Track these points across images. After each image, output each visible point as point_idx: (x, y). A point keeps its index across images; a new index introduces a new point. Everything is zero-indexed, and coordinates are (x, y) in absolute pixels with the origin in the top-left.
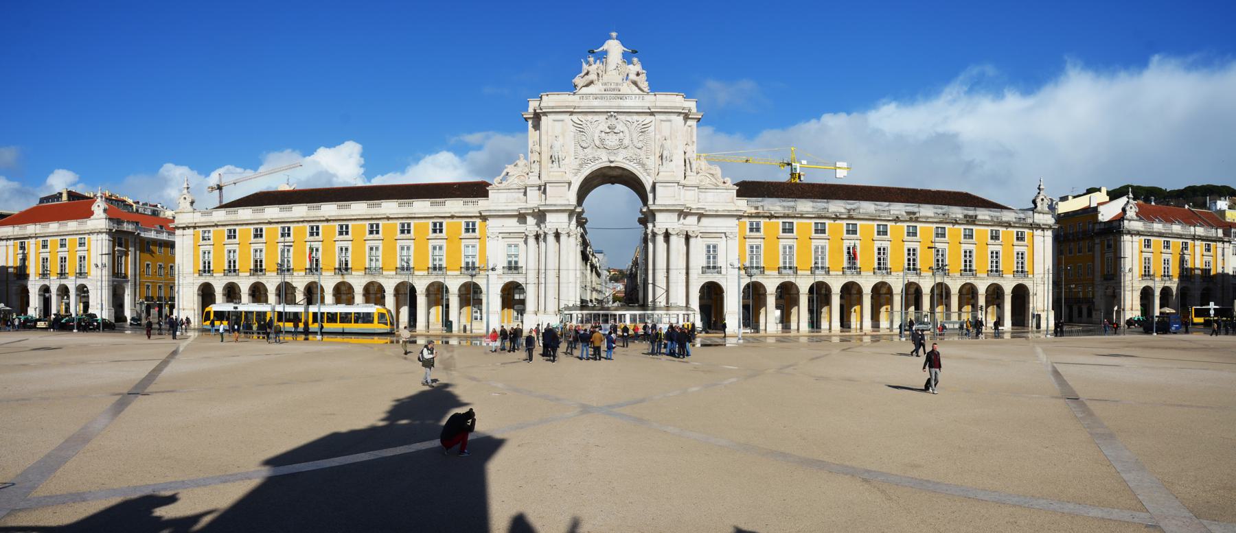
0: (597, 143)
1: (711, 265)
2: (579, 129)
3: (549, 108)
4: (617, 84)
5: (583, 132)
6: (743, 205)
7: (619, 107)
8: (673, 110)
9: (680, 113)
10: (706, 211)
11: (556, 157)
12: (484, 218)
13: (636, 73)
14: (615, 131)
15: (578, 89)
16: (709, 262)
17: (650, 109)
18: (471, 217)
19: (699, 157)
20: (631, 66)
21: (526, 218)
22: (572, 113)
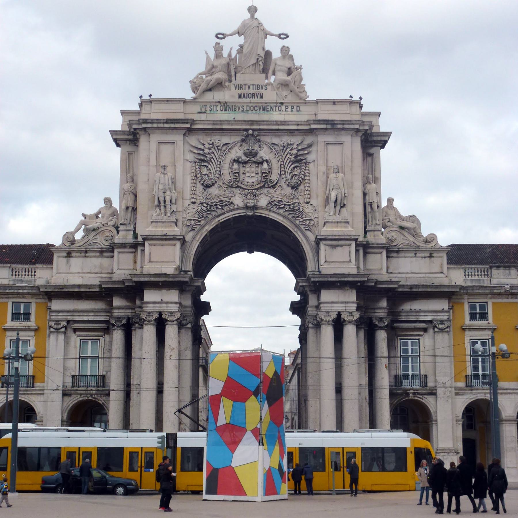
0: (227, 177)
2: (202, 158)
3: (152, 121)
4: (258, 87)
8: (346, 126)
9: (357, 130)
10: (400, 286)
11: (162, 199)
13: (286, 70)
15: (198, 93)
17: (310, 125)
18: (23, 294)
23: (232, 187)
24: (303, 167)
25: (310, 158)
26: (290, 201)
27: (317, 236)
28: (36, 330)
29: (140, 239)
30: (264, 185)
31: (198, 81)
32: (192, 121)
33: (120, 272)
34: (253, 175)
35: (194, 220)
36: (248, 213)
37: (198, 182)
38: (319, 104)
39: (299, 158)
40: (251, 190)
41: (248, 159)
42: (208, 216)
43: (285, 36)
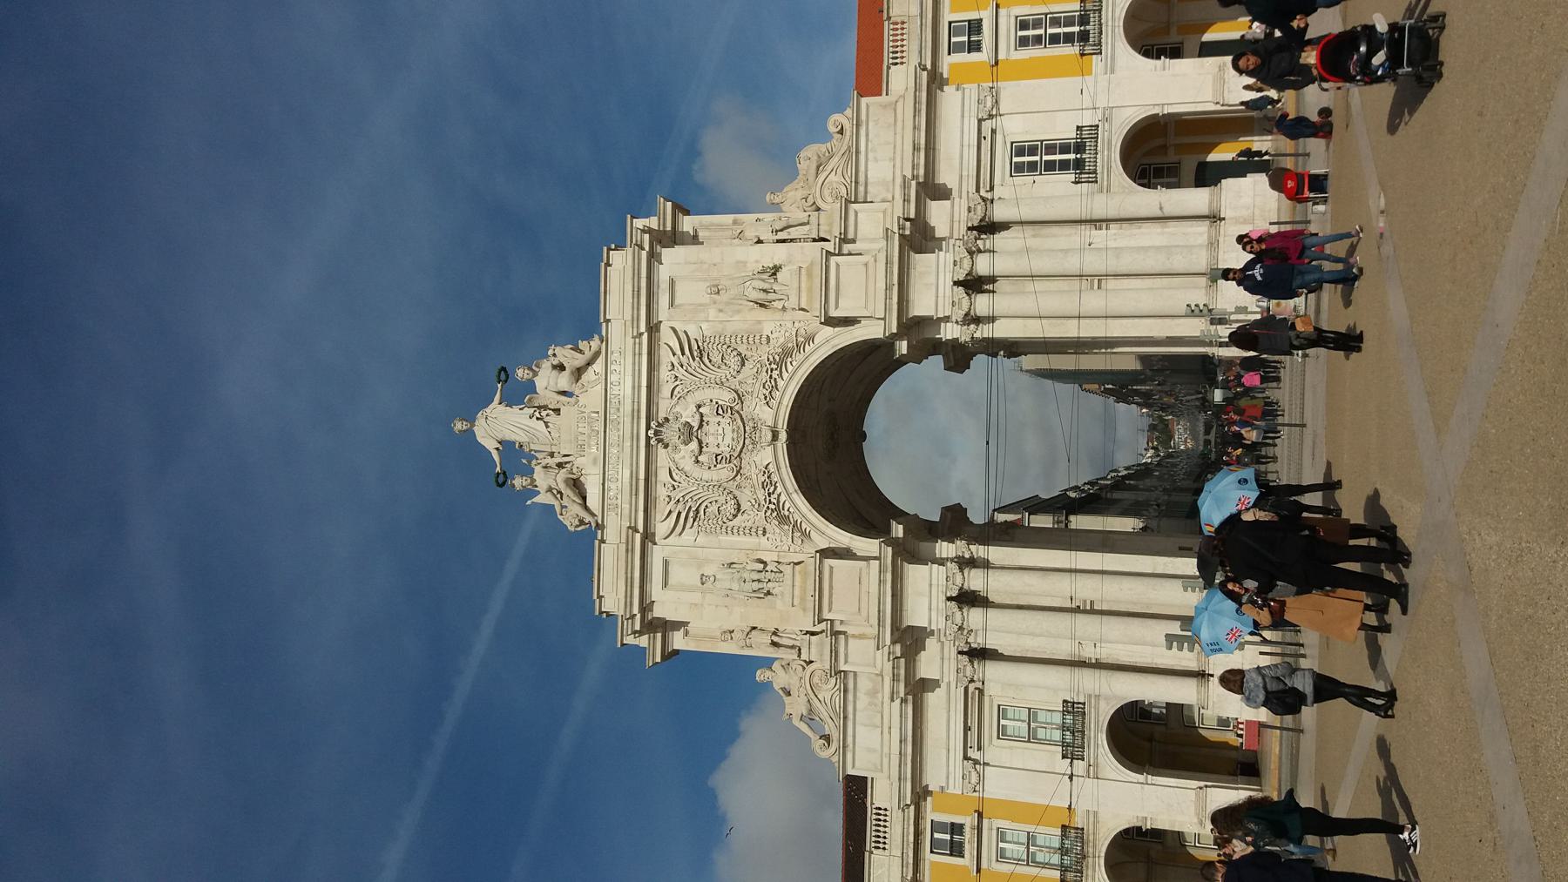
0: (723, 473)
1: (1072, 156)
2: (691, 514)
5: (697, 511)
6: (901, 79)
7: (635, 414)
11: (756, 586)
12: (921, 794)
13: (555, 372)
14: (695, 424)
15: (588, 518)
16: (1064, 165)
17: (641, 334)
19: (776, 207)
20: (540, 383)
21: (923, 680)
22: (648, 537)
23: (741, 468)
24: (710, 346)
25: (694, 333)
26: (765, 369)
27: (821, 323)
28: (980, 815)
29: (823, 626)
30: (738, 412)
31: (570, 518)
32: (630, 531)
33: (879, 663)
34: (721, 432)
35: (793, 532)
36: (784, 440)
37: (731, 524)
38: (608, 318)
39: (695, 354)
40: (746, 435)
41: (694, 438)
42: (786, 509)
43: (502, 372)
